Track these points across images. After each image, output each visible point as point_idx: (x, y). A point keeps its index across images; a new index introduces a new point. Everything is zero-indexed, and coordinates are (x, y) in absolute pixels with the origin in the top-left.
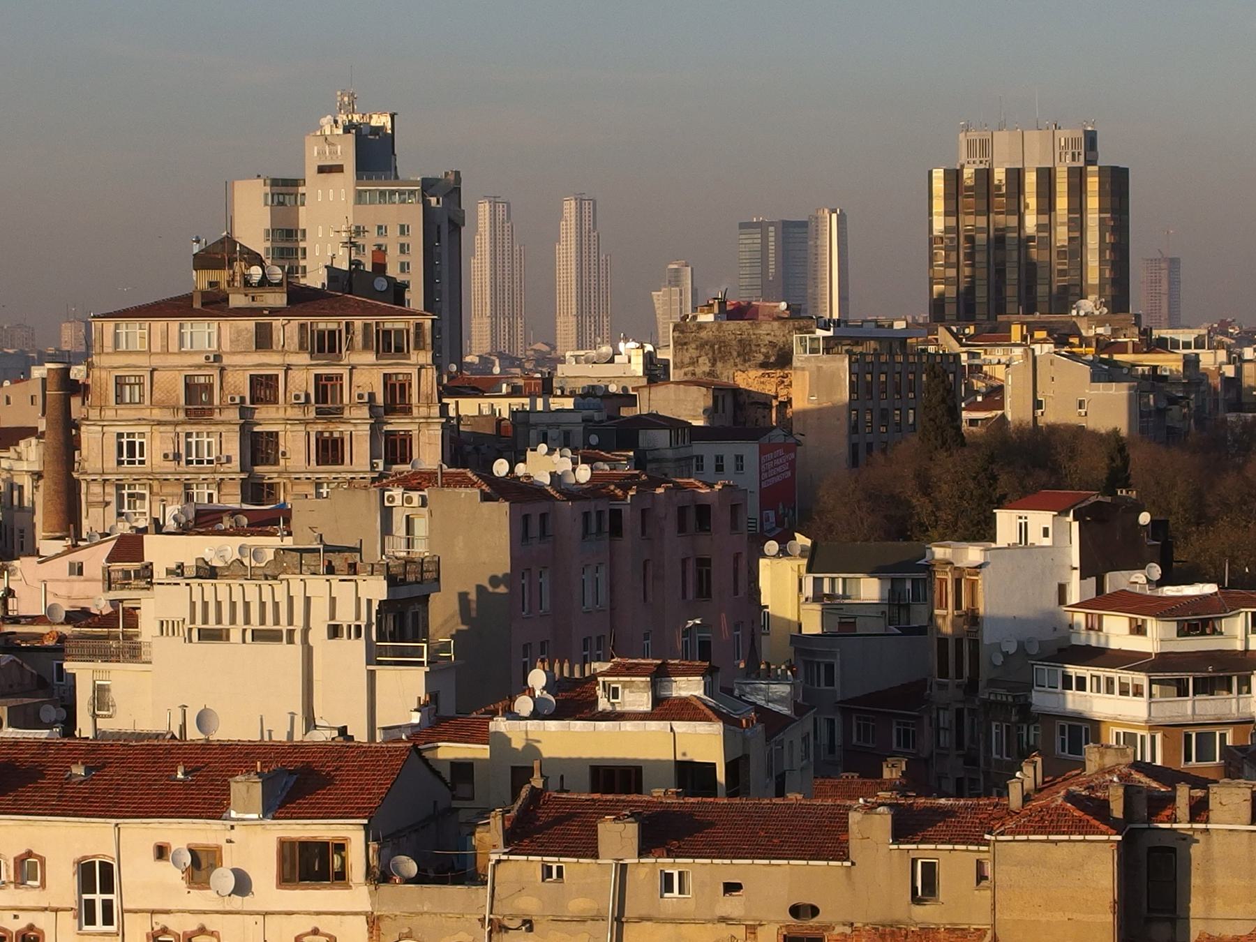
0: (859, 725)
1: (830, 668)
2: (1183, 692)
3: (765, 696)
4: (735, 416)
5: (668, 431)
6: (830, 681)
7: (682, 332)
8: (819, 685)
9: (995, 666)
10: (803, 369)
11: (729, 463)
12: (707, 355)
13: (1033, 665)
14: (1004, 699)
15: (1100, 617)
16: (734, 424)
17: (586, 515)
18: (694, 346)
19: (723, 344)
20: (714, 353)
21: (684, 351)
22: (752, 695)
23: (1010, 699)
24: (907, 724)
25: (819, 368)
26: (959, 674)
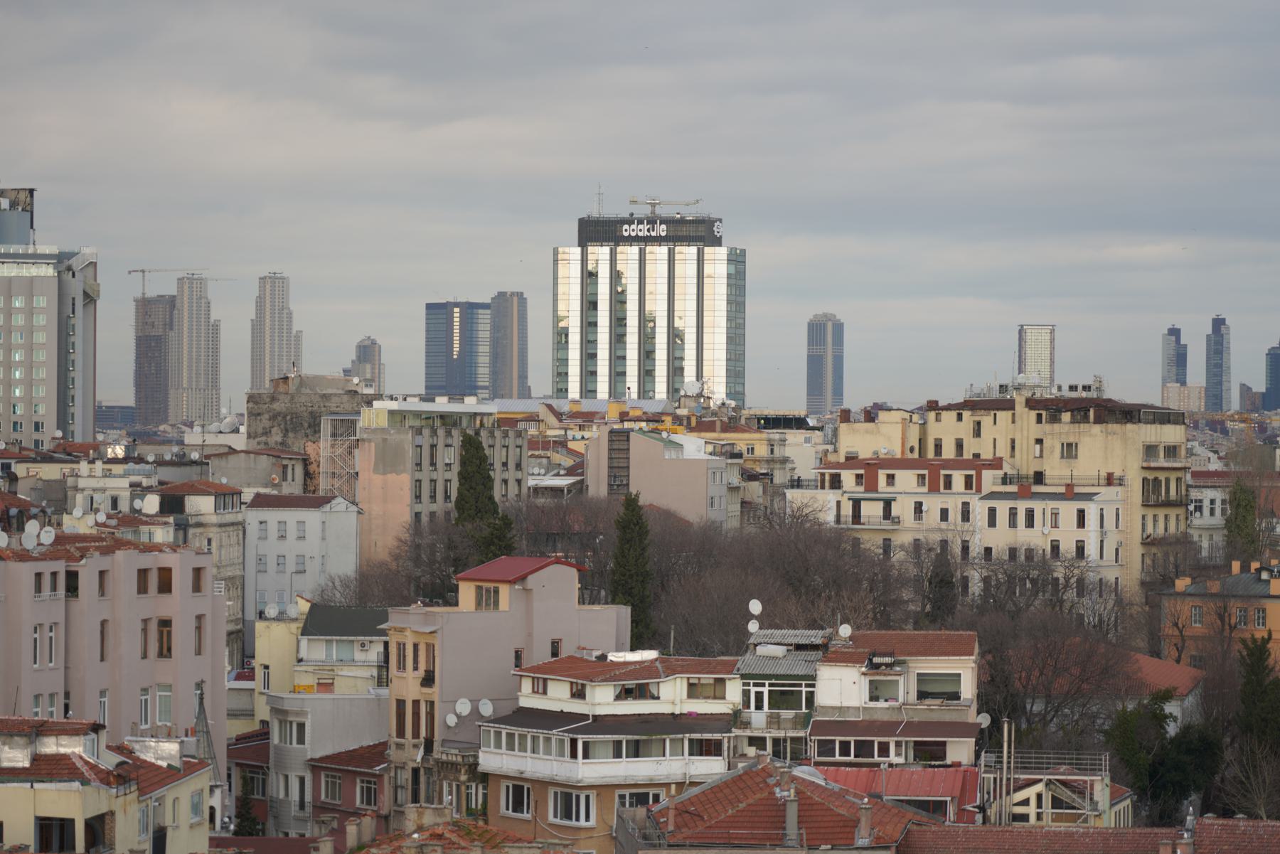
0: (327, 782)
1: (301, 727)
2: (618, 754)
3: (154, 754)
4: (305, 484)
5: (213, 498)
6: (301, 740)
7: (256, 403)
8: (291, 743)
9: (449, 727)
10: (370, 441)
11: (292, 532)
12: (279, 425)
13: (480, 726)
14: (454, 759)
15: (545, 680)
16: (304, 493)
17: (39, 576)
18: (267, 416)
19: (296, 416)
20: (286, 424)
21: (258, 422)
22: (142, 752)
23: (460, 759)
24: (369, 782)
25: (385, 440)
26: (416, 734)
